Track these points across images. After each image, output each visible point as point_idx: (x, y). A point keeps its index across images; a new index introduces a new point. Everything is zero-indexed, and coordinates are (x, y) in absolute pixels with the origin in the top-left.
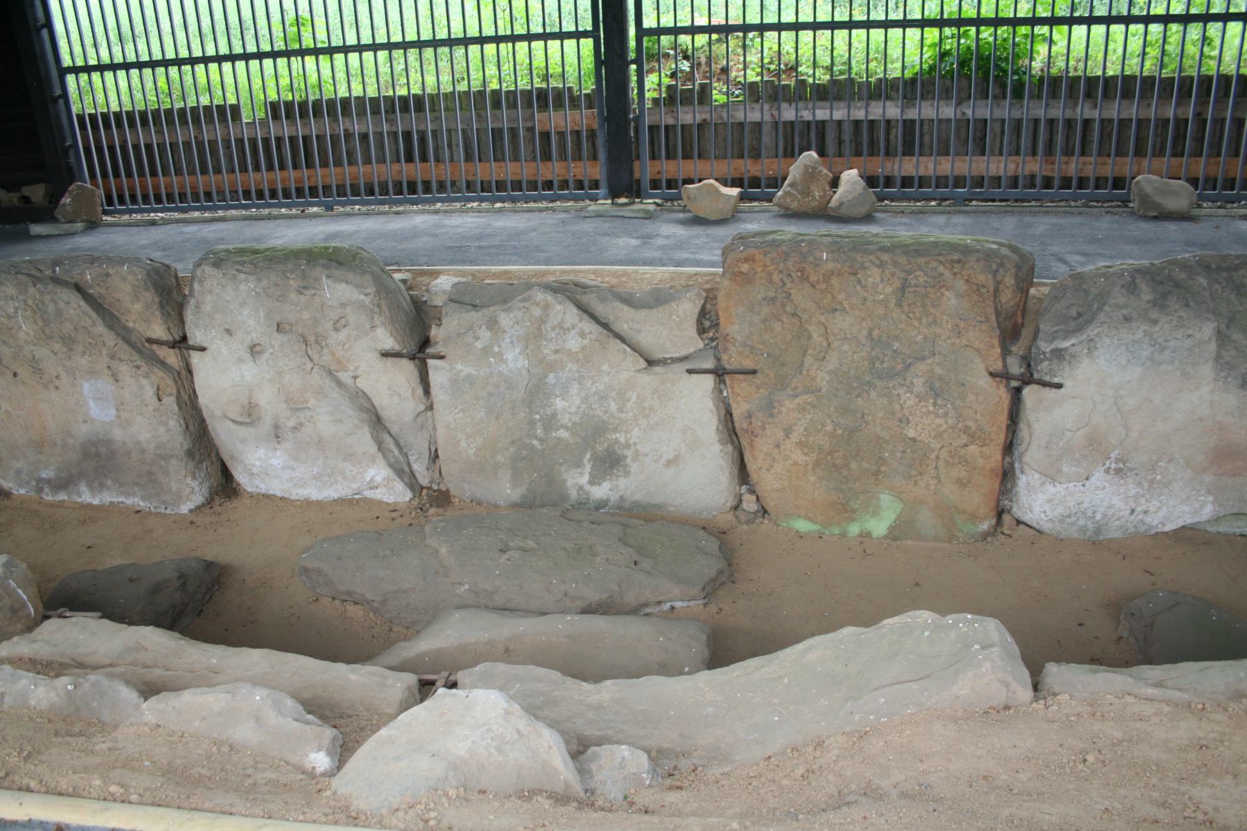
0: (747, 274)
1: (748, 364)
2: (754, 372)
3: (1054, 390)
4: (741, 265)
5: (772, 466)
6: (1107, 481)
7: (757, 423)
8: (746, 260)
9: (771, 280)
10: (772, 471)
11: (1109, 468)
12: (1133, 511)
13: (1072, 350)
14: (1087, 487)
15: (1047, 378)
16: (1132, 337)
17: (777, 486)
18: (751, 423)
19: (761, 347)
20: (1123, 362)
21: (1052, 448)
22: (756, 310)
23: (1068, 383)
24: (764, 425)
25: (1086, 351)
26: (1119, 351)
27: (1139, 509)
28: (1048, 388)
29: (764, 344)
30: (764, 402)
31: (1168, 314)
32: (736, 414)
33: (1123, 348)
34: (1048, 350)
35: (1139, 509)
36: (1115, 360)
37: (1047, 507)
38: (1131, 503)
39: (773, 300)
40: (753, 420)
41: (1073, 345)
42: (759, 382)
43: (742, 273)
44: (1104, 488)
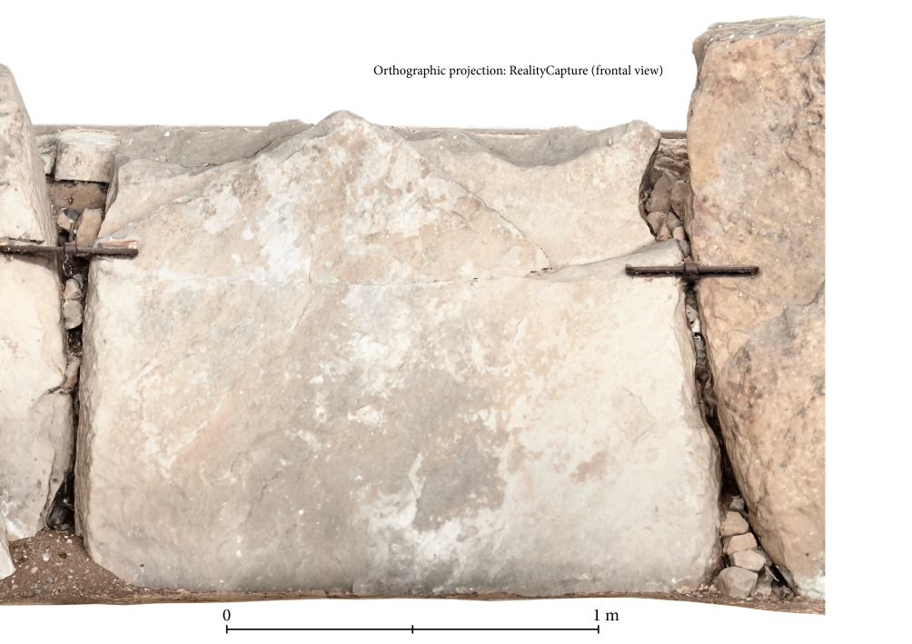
0: (743, 82)
1: (742, 255)
2: (752, 272)
4: (731, 65)
5: (789, 457)
7: (761, 368)
8: (741, 56)
9: (786, 93)
10: (791, 468)
17: (799, 500)
18: (748, 370)
19: (767, 221)
22: (759, 151)
24: (774, 372)
29: (773, 215)
30: (774, 329)
32: (720, 359)
39: (791, 131)
40: (754, 364)
42: (764, 292)
43: (733, 81)
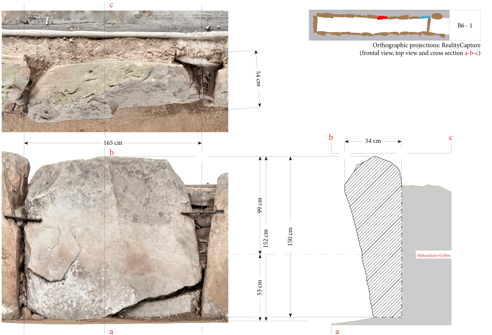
3: (38, 223)
6: (75, 281)
11: (75, 272)
12: (93, 301)
13: (43, 199)
14: (65, 285)
15: (34, 217)
16: (72, 193)
20: (70, 206)
21: (42, 259)
23: (44, 219)
25: (50, 200)
26: (67, 200)
27: (97, 299)
28: (35, 223)
31: (88, 181)
33: (69, 198)
34: (32, 200)
35: (97, 299)
36: (66, 205)
37: (45, 298)
38: (91, 296)
41: (43, 197)
44: (75, 286)
